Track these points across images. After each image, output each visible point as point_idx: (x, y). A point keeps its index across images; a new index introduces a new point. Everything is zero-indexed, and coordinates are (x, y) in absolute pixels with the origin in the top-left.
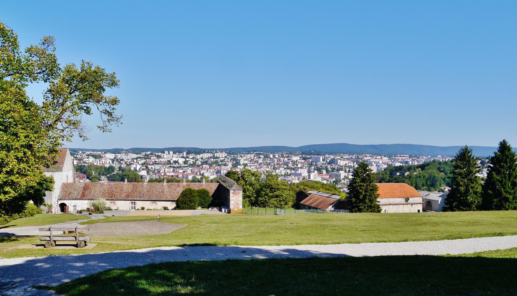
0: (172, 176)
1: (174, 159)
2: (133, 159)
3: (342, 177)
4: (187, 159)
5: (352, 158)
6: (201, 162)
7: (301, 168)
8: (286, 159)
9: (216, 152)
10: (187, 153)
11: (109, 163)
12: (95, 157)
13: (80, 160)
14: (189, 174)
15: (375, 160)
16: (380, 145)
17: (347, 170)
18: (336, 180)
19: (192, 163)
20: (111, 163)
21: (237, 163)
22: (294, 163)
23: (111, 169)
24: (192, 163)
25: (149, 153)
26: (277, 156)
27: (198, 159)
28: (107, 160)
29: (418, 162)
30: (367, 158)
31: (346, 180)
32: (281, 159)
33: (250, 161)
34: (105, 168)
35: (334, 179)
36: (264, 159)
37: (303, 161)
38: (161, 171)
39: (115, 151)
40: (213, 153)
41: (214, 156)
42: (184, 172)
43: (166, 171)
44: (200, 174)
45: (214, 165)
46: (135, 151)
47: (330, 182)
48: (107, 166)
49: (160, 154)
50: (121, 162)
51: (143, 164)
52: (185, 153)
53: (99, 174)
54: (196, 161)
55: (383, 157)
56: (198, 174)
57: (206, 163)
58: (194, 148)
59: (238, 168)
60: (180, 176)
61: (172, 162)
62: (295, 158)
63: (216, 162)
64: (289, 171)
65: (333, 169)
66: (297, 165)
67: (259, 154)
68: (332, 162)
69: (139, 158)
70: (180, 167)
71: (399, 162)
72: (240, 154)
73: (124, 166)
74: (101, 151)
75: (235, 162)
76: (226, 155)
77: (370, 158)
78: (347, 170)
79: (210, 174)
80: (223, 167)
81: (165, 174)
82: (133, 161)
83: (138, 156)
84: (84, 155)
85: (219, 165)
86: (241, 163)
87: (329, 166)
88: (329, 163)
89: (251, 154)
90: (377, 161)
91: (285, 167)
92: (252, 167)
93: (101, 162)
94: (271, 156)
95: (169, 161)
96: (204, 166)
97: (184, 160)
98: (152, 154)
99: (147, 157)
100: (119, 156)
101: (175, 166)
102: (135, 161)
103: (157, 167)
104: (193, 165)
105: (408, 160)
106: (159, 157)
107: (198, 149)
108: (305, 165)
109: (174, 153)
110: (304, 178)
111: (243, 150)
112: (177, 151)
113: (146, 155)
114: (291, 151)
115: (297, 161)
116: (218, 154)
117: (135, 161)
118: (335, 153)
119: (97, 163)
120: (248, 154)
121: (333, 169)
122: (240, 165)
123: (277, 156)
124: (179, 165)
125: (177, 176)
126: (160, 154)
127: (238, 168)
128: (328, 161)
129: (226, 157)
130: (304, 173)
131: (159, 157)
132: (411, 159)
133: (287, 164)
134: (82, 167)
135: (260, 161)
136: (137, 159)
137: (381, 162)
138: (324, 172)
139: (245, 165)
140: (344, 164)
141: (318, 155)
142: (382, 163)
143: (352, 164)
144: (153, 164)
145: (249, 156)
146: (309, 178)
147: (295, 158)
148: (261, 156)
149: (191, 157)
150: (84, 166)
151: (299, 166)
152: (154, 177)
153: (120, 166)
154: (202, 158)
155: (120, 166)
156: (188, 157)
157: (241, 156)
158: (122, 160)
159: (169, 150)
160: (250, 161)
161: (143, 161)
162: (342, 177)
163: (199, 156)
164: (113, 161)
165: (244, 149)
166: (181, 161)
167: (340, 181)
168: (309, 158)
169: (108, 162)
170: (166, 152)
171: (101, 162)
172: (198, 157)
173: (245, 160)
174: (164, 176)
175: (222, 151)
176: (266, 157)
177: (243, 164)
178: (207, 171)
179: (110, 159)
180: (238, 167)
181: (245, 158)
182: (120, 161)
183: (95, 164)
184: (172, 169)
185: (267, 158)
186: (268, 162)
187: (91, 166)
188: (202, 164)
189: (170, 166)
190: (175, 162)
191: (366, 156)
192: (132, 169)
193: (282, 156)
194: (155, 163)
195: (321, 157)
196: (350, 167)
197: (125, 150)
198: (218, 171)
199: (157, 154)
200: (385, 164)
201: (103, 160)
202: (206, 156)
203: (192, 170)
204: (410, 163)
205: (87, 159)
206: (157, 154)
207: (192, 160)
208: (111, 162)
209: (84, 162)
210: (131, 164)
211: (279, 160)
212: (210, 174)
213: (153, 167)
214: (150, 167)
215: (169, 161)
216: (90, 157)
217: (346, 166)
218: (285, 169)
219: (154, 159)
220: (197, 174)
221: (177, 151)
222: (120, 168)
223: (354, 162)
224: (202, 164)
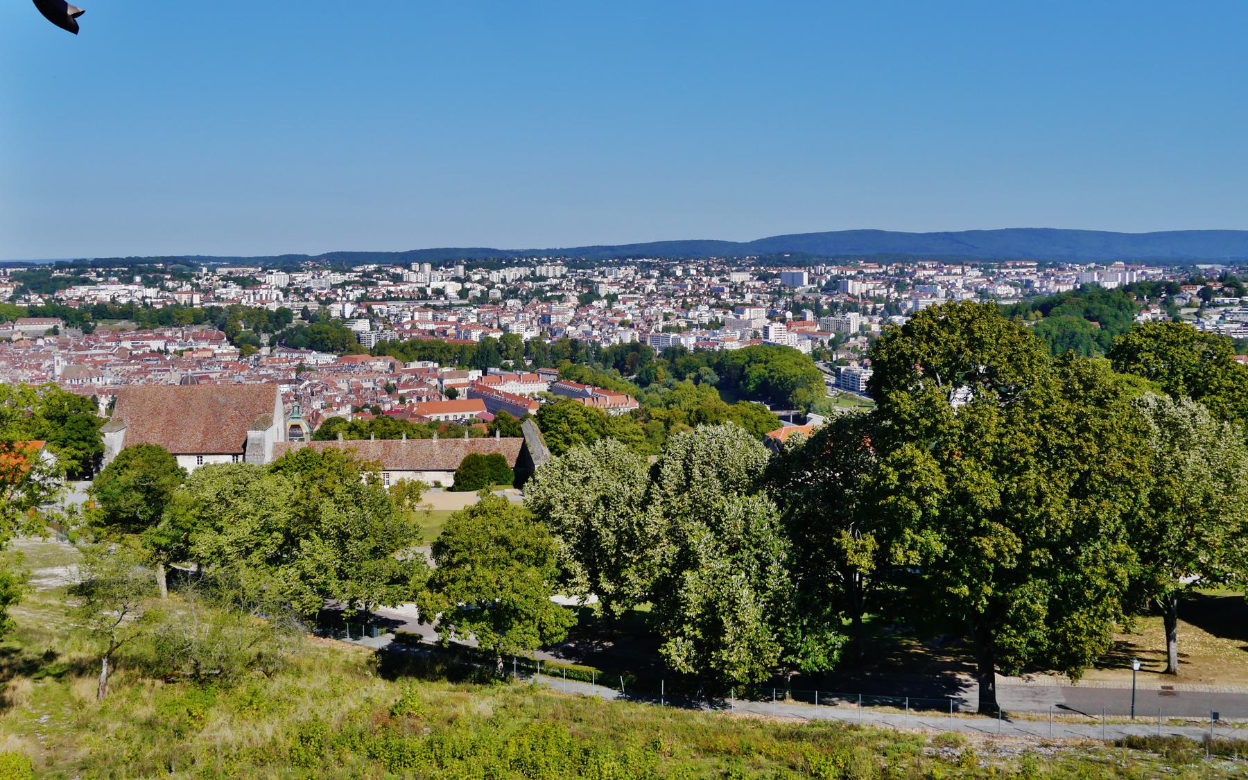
0: (432, 332)
1: (436, 284)
2: (334, 287)
3: (854, 329)
4: (468, 285)
5: (885, 273)
6: (502, 290)
7: (753, 305)
8: (716, 280)
9: (541, 263)
10: (468, 268)
11: (277, 299)
12: (244, 283)
13: (207, 291)
14: (473, 326)
15: (946, 278)
16: (968, 233)
17: (870, 307)
18: (838, 336)
19: (479, 295)
20: (281, 298)
21: (590, 292)
22: (737, 290)
23: (283, 315)
24: (479, 295)
25: (372, 267)
26: (693, 272)
27: (493, 284)
28: (271, 292)
29: (1057, 282)
30: (926, 273)
31: (860, 338)
32: (704, 279)
33: (625, 287)
34: (269, 313)
35: (832, 336)
36: (660, 282)
37: (758, 284)
38: (405, 320)
39: (290, 264)
40: (530, 266)
41: (533, 273)
42: (460, 320)
43: (416, 318)
44: (499, 326)
45: (534, 300)
46: (341, 261)
47: (822, 343)
48: (274, 307)
49: (399, 270)
50: (307, 295)
51: (358, 301)
52: (461, 268)
53: (256, 330)
54: (489, 288)
55: (967, 269)
56: (495, 326)
57: (511, 293)
58: (483, 250)
59: (593, 307)
60: (451, 331)
61: (429, 292)
62: (737, 277)
63: (539, 292)
64: (720, 315)
65: (834, 306)
66: (743, 296)
67: (648, 265)
68: (835, 285)
69: (349, 283)
70: (448, 308)
71: (1006, 283)
72: (601, 265)
73: (313, 306)
75: (585, 291)
76: (565, 270)
77: (932, 273)
78: (870, 307)
79: (523, 327)
80: (556, 306)
81: (414, 327)
82: (335, 292)
83: (346, 278)
84: (216, 278)
85: (548, 300)
86: (603, 293)
87: (824, 297)
88: (825, 290)
89: (629, 264)
90: (952, 279)
91: (713, 301)
92: (629, 304)
93: (258, 297)
94: (679, 273)
95: (423, 290)
96: (510, 302)
97: (459, 286)
98: (379, 271)
99: (367, 281)
100: (299, 279)
101: (438, 303)
102: (340, 291)
103: (393, 308)
104: (482, 300)
105: (1032, 278)
106: (397, 279)
107: (494, 251)
108: (763, 296)
109: (435, 267)
110: (756, 334)
111: (608, 253)
112: (441, 259)
113: (365, 274)
114: (731, 255)
115: (743, 283)
116: (544, 268)
117: (340, 291)
118: (847, 257)
119: (249, 300)
120: (619, 266)
121: (834, 306)
122: (598, 298)
123: (693, 272)
124: (447, 302)
125: (444, 333)
126: (399, 270)
127: (593, 307)
128: (824, 283)
129: (563, 276)
130: (757, 317)
131: (397, 279)
132: (1041, 274)
133: (716, 293)
134: (215, 313)
135: (650, 286)
136: (343, 285)
137: (959, 284)
138: (810, 316)
139: (612, 298)
140: (864, 291)
141: (799, 266)
142: (965, 287)
143: (883, 292)
144: (383, 300)
145: (622, 272)
146: (766, 335)
147: (737, 277)
148: (651, 272)
149: (477, 277)
150: (219, 309)
151: (749, 297)
152: (389, 335)
153: (306, 307)
154: (504, 281)
155: (306, 307)
156: (468, 279)
157: (602, 273)
158: (309, 290)
159: (421, 256)
160: (625, 287)
161: (358, 293)
162: (854, 329)
163: (494, 273)
164: (286, 292)
165: (611, 248)
166: (452, 289)
167: (847, 339)
168: (776, 276)
169: (274, 297)
170: (415, 266)
171: (258, 297)
172: (495, 276)
173: (611, 284)
174: (411, 331)
175: (553, 255)
176: (666, 273)
177: (607, 296)
178: (517, 319)
180: (595, 303)
181: (611, 278)
182: (302, 293)
183: (244, 302)
184: (430, 314)
185: (669, 276)
186: (671, 287)
187: (235, 308)
188: (505, 298)
189: (426, 306)
190: (439, 292)
191: (924, 268)
192: (335, 313)
193: (708, 273)
194: (389, 298)
195: (806, 275)
196: (878, 299)
197: (313, 259)
198: (543, 315)
199: (392, 270)
200: (969, 289)
201: (263, 292)
202: (512, 274)
203: (478, 315)
204: (1037, 284)
205: (224, 290)
206: (392, 270)
207: (480, 287)
208: (281, 295)
209: (217, 299)
210: (329, 301)
211: (698, 282)
212: (523, 327)
213: (384, 307)
214: (376, 308)
215: (423, 290)
217: (866, 296)
218: (711, 307)
219: (385, 286)
220: (491, 327)
221: (441, 259)
222: (305, 313)
223: (889, 286)
224: (505, 298)
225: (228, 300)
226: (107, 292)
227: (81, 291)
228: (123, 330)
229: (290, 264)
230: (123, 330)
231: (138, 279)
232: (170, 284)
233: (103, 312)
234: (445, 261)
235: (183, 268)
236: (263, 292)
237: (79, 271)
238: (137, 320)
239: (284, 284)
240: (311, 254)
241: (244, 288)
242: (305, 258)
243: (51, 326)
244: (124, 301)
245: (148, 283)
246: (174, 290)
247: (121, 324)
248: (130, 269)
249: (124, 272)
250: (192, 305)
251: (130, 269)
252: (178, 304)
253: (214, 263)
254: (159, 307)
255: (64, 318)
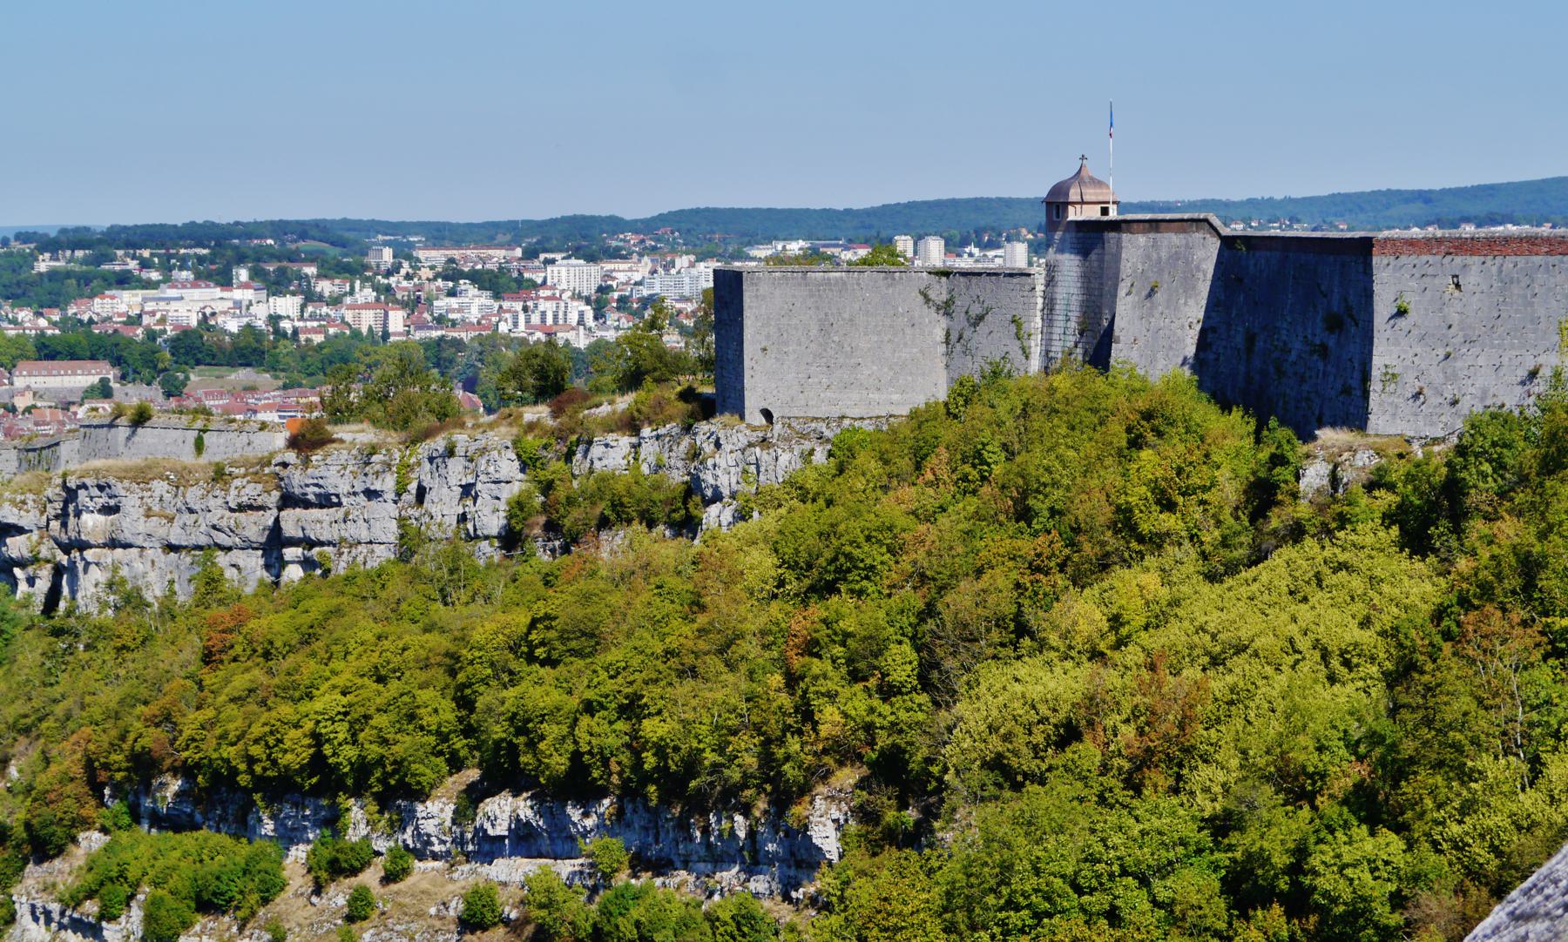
12: (494, 283)
25: (795, 247)
39: (587, 238)
74: (511, 232)
93: (535, 319)
100: (622, 277)
111: (1417, 208)
119: (517, 323)
150: (458, 344)
169: (573, 318)
179: (577, 296)
183: (503, 328)
205: (453, 302)
209: (440, 321)
216: (464, 284)
225: (467, 325)
226: (185, 304)
227: (125, 302)
228: (251, 389)
229: (587, 238)
230: (251, 389)
231: (243, 274)
232: (325, 287)
233: (197, 347)
234: (979, 233)
235: (340, 249)
236: (548, 307)
237: (103, 255)
238: (273, 368)
239: (589, 289)
240: (628, 215)
241: (497, 296)
242: (616, 225)
243: (95, 379)
244: (233, 326)
245: (276, 285)
246: (336, 301)
247: (242, 375)
248: (218, 251)
249: (201, 260)
250: (386, 335)
251: (218, 251)
252: (356, 334)
253: (402, 236)
254: (318, 339)
255: (117, 361)
